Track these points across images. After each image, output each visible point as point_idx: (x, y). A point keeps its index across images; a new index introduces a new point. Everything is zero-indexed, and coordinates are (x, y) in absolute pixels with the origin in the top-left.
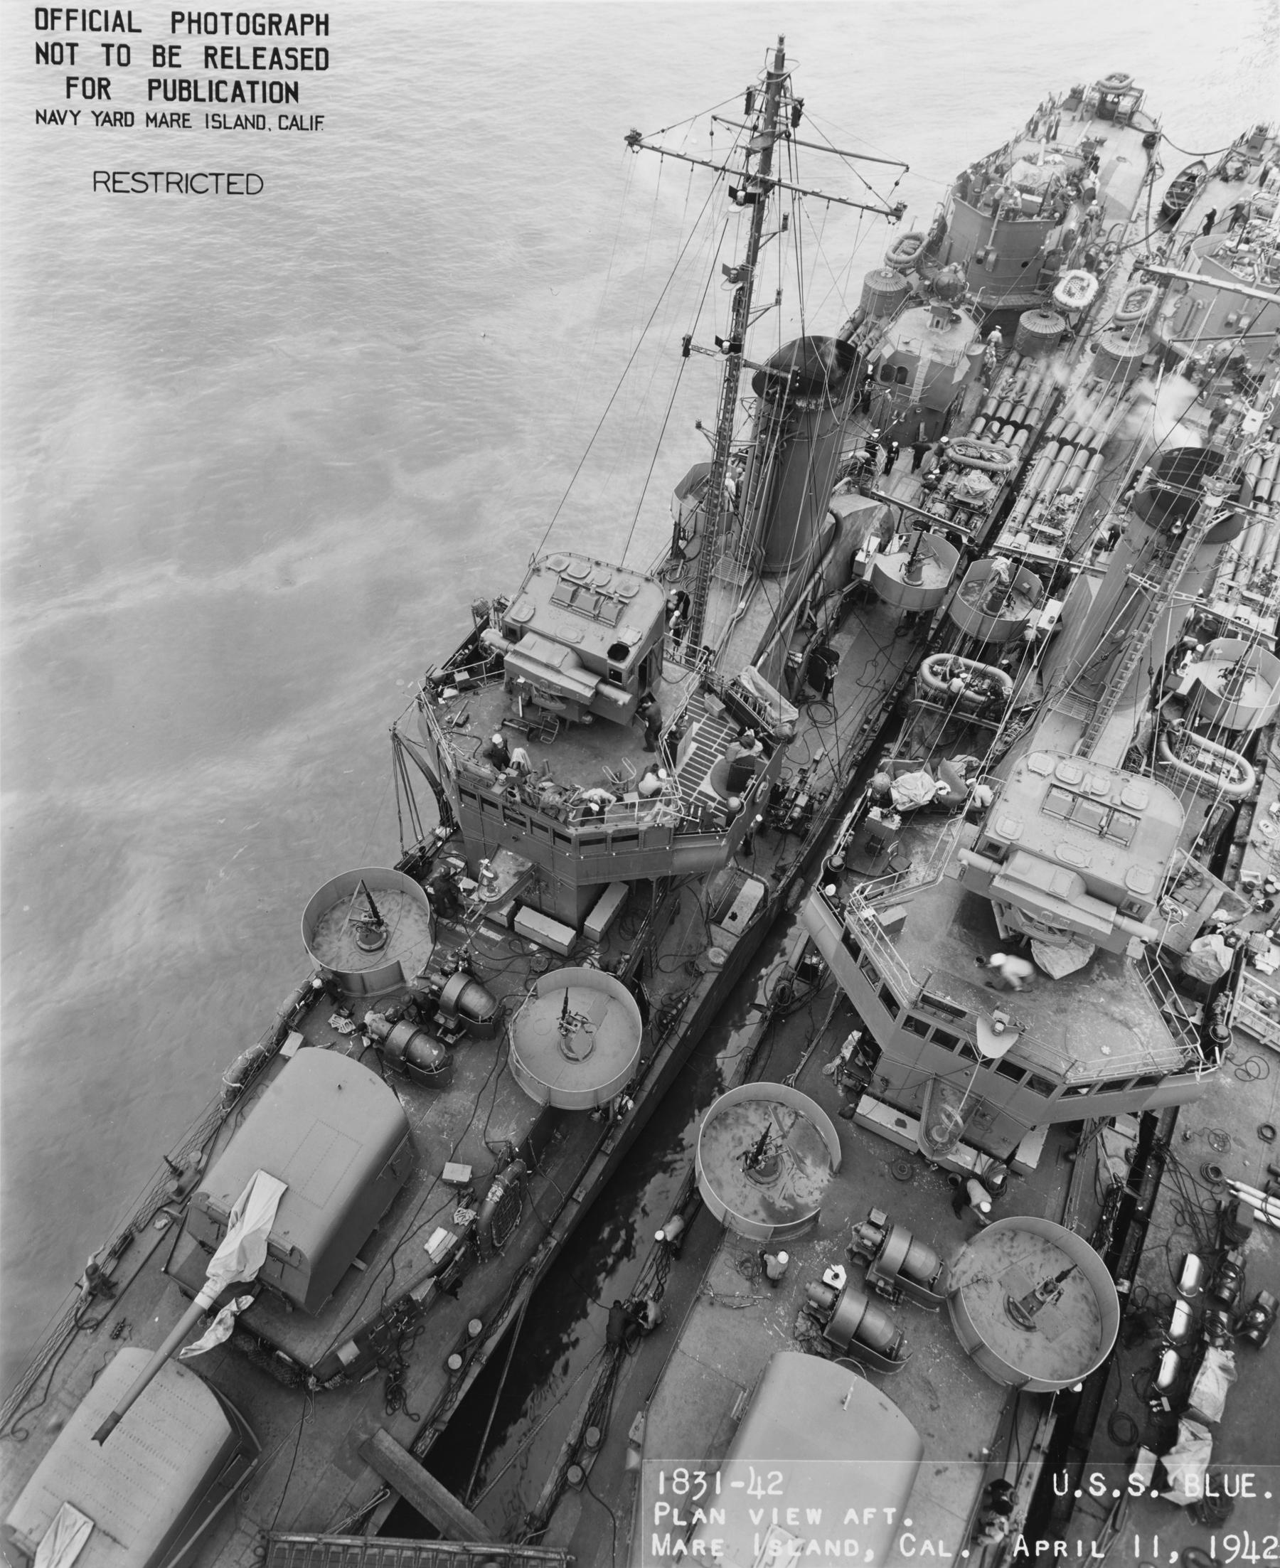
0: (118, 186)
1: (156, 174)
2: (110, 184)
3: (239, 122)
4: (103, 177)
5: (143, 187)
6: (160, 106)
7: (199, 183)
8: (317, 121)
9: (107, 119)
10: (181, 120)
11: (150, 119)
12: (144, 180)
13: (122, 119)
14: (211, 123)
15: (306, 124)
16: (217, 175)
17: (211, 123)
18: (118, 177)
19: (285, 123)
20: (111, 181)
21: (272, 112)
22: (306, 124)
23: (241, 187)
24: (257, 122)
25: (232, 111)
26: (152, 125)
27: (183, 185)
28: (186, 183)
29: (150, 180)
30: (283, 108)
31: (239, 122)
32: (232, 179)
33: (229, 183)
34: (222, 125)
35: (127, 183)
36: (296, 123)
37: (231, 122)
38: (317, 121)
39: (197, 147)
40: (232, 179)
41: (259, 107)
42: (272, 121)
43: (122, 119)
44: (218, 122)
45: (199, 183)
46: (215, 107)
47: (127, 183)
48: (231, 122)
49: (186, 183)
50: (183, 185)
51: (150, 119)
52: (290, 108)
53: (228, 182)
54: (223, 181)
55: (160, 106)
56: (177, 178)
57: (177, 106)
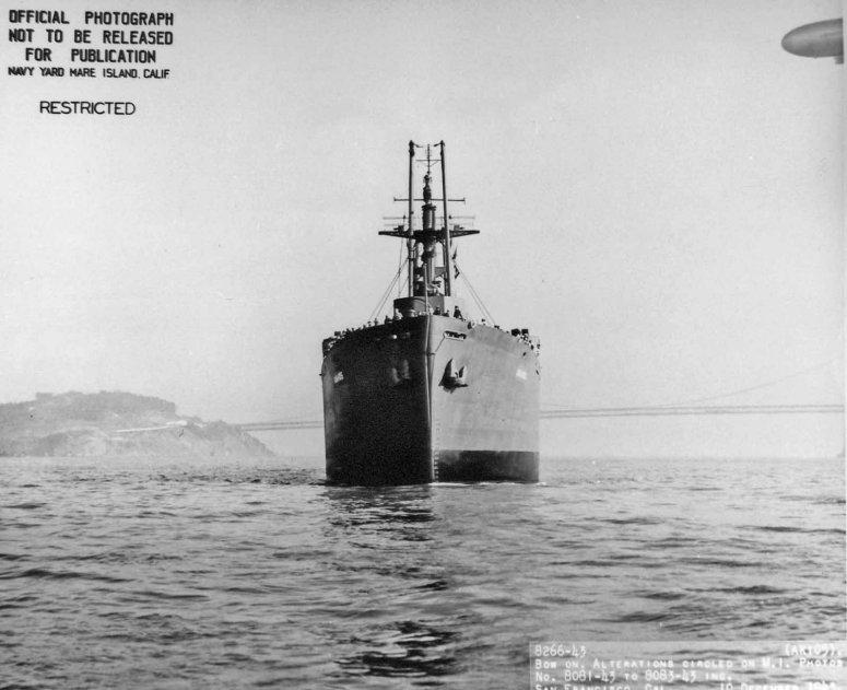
1: (75, 103)
3: (123, 74)
5: (67, 110)
6: (78, 64)
7: (99, 108)
8: (165, 73)
10: (90, 72)
11: (73, 72)
12: (69, 107)
13: (57, 72)
15: (159, 75)
16: (109, 103)
19: (148, 74)
21: (140, 67)
22: (159, 75)
23: (122, 109)
24: (132, 74)
25: (119, 67)
28: (92, 108)
29: (72, 106)
30: (147, 65)
31: (123, 74)
32: (118, 106)
33: (116, 108)
34: (113, 75)
35: (59, 108)
36: (154, 74)
37: (117, 74)
38: (165, 73)
39: (97, 88)
40: (118, 106)
42: (140, 73)
43: (57, 72)
44: (110, 74)
46: (108, 65)
47: (59, 108)
48: (117, 74)
49: (92, 108)
51: (73, 72)
52: (151, 66)
53: (115, 107)
54: (113, 106)
55: (78, 64)
56: (85, 105)
57: (88, 65)
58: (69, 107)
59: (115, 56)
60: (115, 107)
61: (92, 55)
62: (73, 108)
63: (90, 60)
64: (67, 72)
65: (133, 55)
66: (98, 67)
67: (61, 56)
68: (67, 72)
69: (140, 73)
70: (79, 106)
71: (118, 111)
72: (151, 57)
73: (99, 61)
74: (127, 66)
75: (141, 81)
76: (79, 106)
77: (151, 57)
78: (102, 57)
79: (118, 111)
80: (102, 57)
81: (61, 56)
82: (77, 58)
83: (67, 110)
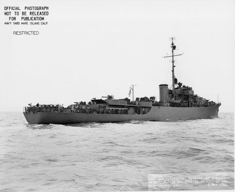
0: (17, 34)
5: (20, 34)
6: (23, 21)
7: (29, 33)
8: (47, 23)
10: (27, 23)
12: (21, 33)
13: (18, 23)
19: (42, 23)
20: (16, 33)
21: (40, 22)
23: (35, 33)
24: (38, 23)
25: (34, 22)
27: (27, 33)
28: (27, 33)
30: (42, 21)
36: (43, 23)
38: (47, 23)
39: (29, 27)
41: (38, 21)
42: (40, 23)
43: (18, 23)
44: (32, 23)
45: (29, 33)
46: (32, 21)
47: (18, 33)
49: (27, 33)
50: (27, 33)
52: (43, 21)
53: (34, 33)
54: (33, 32)
55: (23, 21)
56: (25, 32)
57: (26, 21)
58: (21, 33)
59: (33, 19)
60: (34, 33)
61: (27, 19)
62: (22, 34)
64: (20, 23)
65: (38, 18)
66: (29, 22)
67: (19, 19)
68: (20, 23)
72: (43, 19)
73: (29, 20)
74: (36, 21)
75: (40, 25)
77: (43, 19)
78: (30, 19)
80: (30, 19)
81: (19, 19)
82: (23, 19)
83: (20, 34)
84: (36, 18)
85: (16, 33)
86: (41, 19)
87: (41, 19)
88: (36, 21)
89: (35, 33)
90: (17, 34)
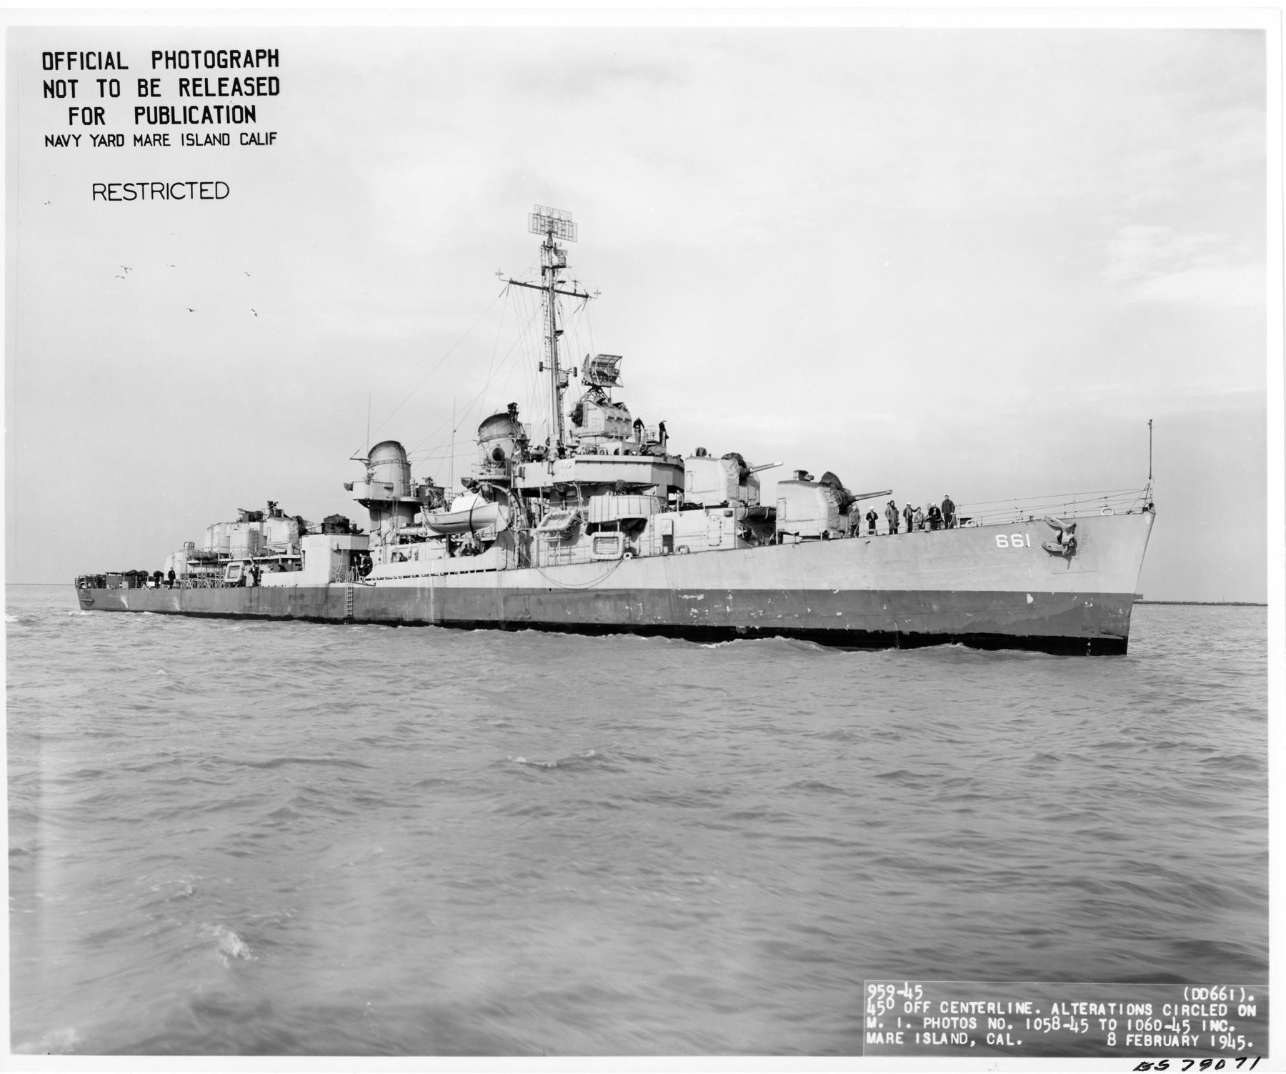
0: (113, 196)
2: (106, 194)
3: (209, 140)
4: (100, 188)
5: (131, 195)
6: (145, 128)
7: (178, 191)
8: (271, 137)
9: (102, 141)
10: (163, 139)
12: (132, 191)
13: (114, 140)
14: (186, 141)
15: (263, 140)
17: (186, 141)
18: (112, 188)
19: (246, 139)
20: (106, 191)
21: (234, 130)
22: (263, 140)
23: (211, 191)
24: (223, 140)
25: (203, 130)
26: (138, 144)
27: (164, 193)
28: (167, 191)
29: (138, 189)
30: (243, 127)
31: (209, 140)
32: (204, 187)
35: (120, 193)
37: (202, 141)
38: (271, 137)
39: (176, 161)
40: (204, 187)
42: (235, 139)
43: (114, 140)
44: (192, 140)
45: (178, 191)
46: (189, 128)
47: (120, 193)
48: (202, 141)
49: (167, 191)
50: (164, 193)
52: (249, 127)
53: (201, 189)
54: (197, 188)
55: (145, 128)
56: (157, 187)
57: (159, 129)
58: (132, 191)
59: (197, 115)
60: (201, 189)
61: (164, 114)
63: (162, 122)
64: (129, 140)
65: (223, 111)
66: (174, 132)
67: (119, 116)
68: (129, 140)
69: (235, 139)
70: (147, 188)
71: (204, 194)
72: (251, 114)
73: (174, 122)
74: (215, 129)
76: (148, 188)
77: (251, 114)
78: (179, 116)
79: (204, 194)
80: (179, 116)
81: (119, 116)
83: (131, 195)
84: (214, 113)
85: (106, 191)
86: (238, 118)
87: (238, 118)
88: (215, 129)
89: (211, 193)
90: (113, 196)
